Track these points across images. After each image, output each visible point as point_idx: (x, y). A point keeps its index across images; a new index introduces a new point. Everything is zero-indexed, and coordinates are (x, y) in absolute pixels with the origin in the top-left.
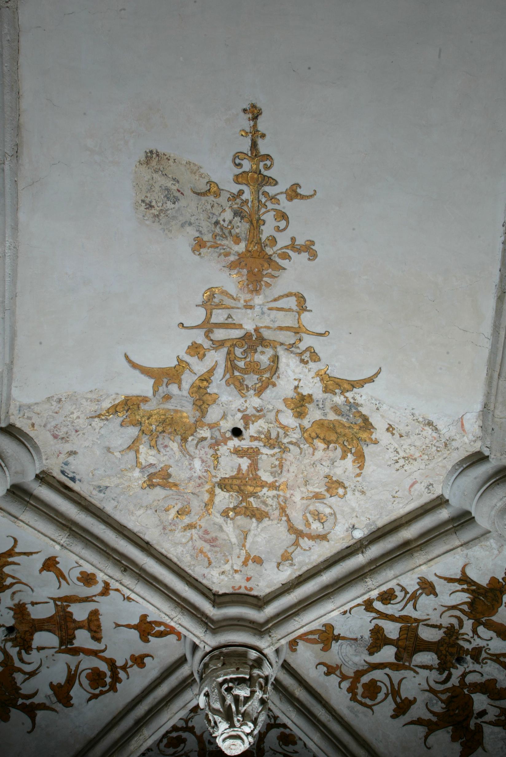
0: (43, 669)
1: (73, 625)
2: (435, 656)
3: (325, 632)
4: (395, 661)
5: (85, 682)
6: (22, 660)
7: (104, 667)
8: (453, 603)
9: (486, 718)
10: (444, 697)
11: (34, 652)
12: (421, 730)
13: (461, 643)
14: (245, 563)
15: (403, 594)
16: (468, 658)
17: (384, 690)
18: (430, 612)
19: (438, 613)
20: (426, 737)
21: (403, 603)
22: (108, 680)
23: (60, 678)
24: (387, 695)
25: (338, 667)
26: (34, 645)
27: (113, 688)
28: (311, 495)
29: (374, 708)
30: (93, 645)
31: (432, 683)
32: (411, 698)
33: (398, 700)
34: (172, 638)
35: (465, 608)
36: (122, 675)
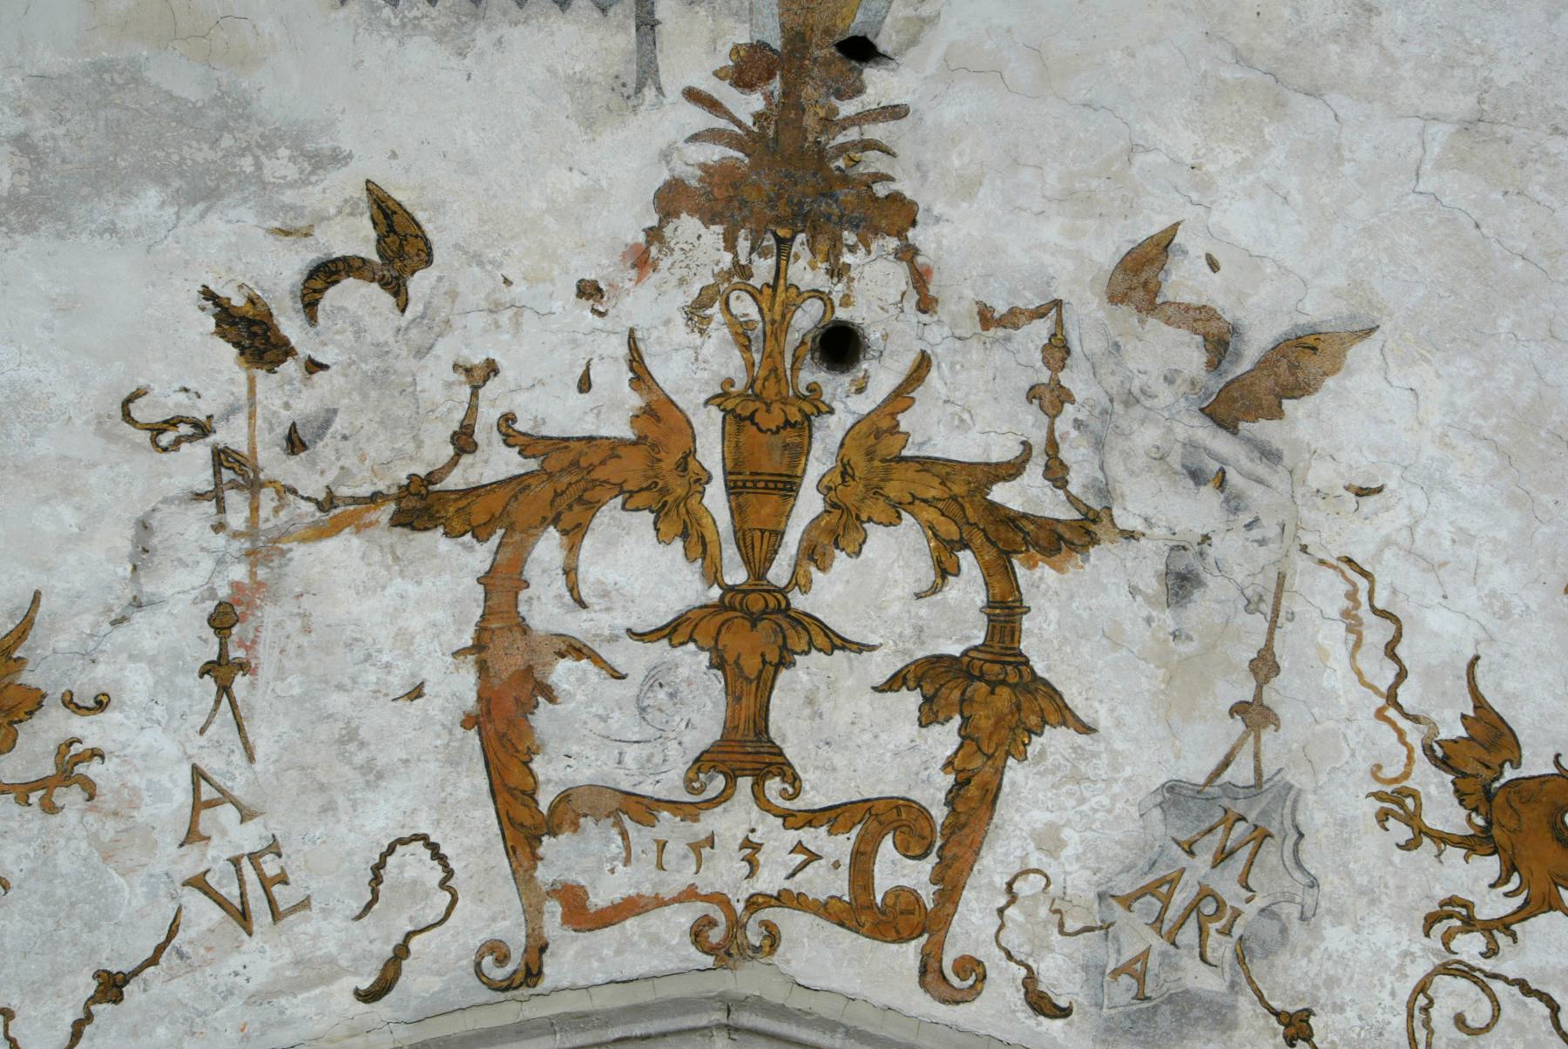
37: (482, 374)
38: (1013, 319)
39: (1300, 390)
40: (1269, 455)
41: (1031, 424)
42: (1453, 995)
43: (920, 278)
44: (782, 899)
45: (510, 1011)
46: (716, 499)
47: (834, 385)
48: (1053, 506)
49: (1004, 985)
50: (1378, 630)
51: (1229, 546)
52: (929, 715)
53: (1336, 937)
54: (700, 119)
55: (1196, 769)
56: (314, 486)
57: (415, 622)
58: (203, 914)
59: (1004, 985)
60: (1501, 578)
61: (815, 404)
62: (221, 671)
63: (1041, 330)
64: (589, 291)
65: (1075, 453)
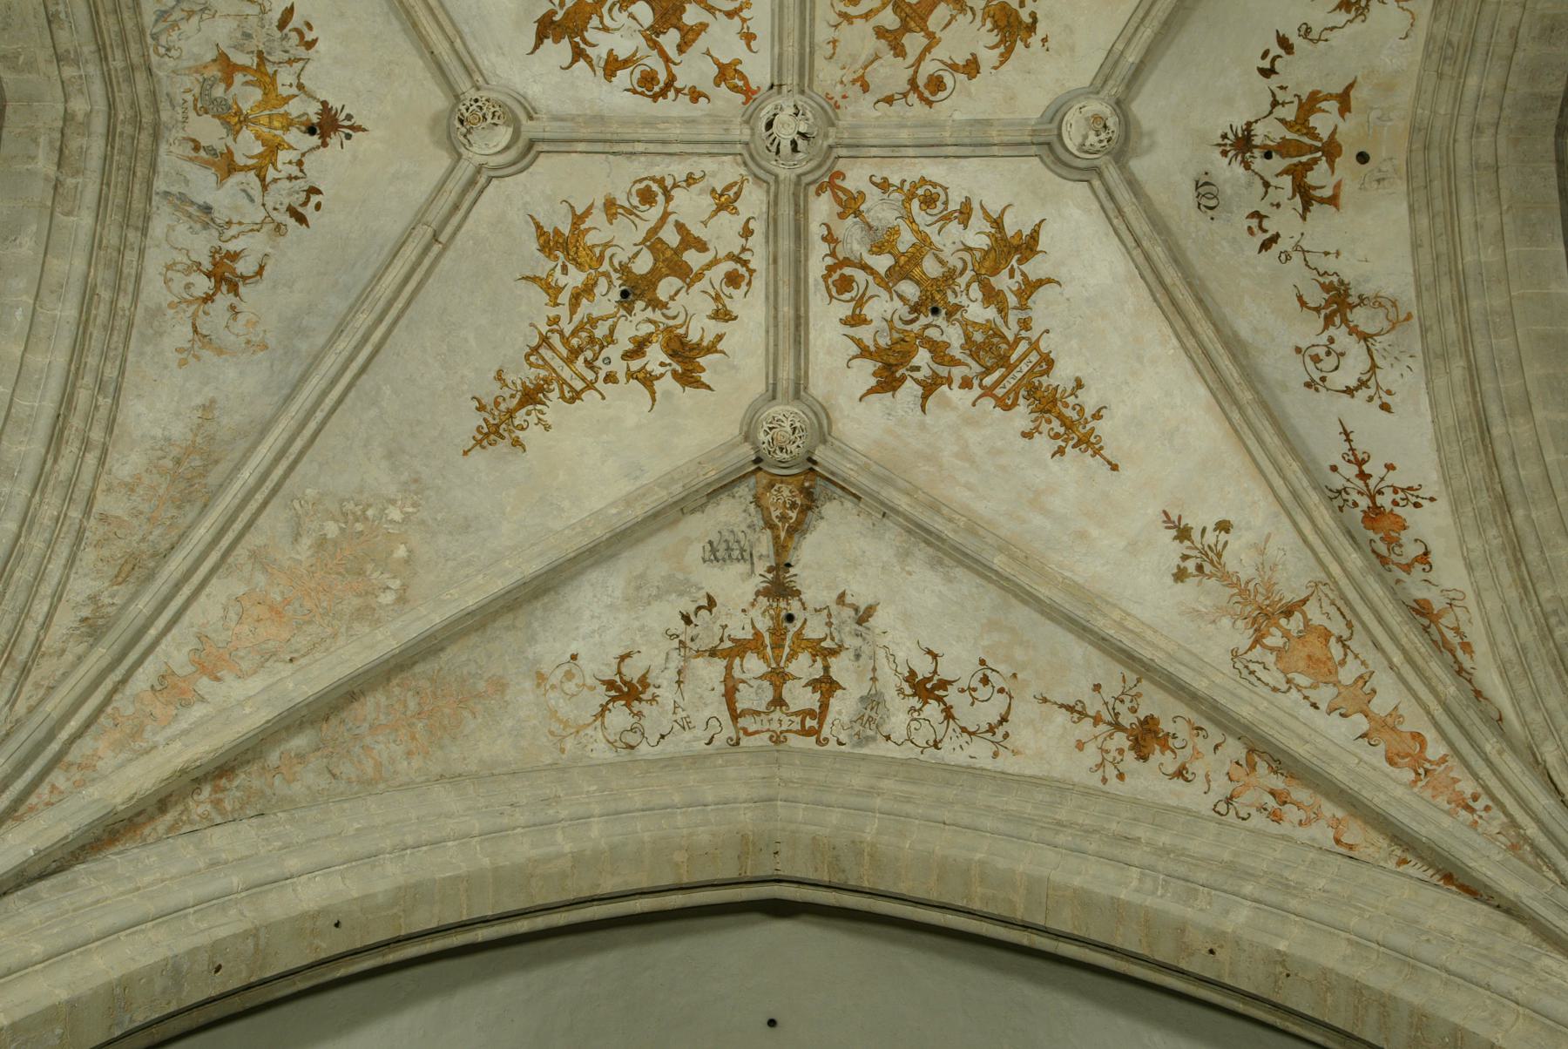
0: (617, 34)
1: (674, 21)
2: (918, 294)
3: (854, 199)
4: (883, 274)
5: (637, 74)
6: (610, 10)
7: (662, 77)
8: (972, 245)
9: (916, 375)
10: (896, 336)
11: (625, 14)
12: (855, 350)
13: (949, 293)
14: (854, 82)
15: (942, 207)
16: (943, 311)
17: (853, 294)
18: (949, 244)
19: (954, 248)
20: (855, 357)
21: (935, 218)
22: (657, 89)
23: (622, 54)
24: (852, 299)
25: (836, 241)
26: (630, 10)
27: (655, 98)
28: (949, 62)
29: (834, 301)
30: (672, 52)
31: (896, 317)
32: (869, 318)
33: (857, 312)
34: (741, 98)
35: (978, 255)
36: (671, 94)
37: (724, 627)
38: (820, 610)
39: (870, 616)
40: (868, 629)
41: (826, 630)
42: (914, 724)
43: (803, 604)
44: (787, 731)
45: (734, 749)
46: (769, 650)
47: (789, 626)
48: (833, 646)
49: (833, 741)
50: (891, 659)
51: (865, 648)
52: (814, 691)
53: (893, 719)
54: (762, 579)
55: (865, 693)
56: (695, 648)
57: (713, 675)
58: (677, 727)
59: (833, 741)
60: (908, 644)
61: (787, 630)
62: (679, 682)
63: (826, 611)
64: (744, 611)
65: (835, 634)
